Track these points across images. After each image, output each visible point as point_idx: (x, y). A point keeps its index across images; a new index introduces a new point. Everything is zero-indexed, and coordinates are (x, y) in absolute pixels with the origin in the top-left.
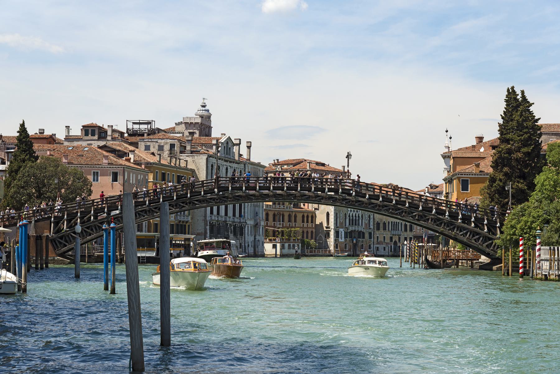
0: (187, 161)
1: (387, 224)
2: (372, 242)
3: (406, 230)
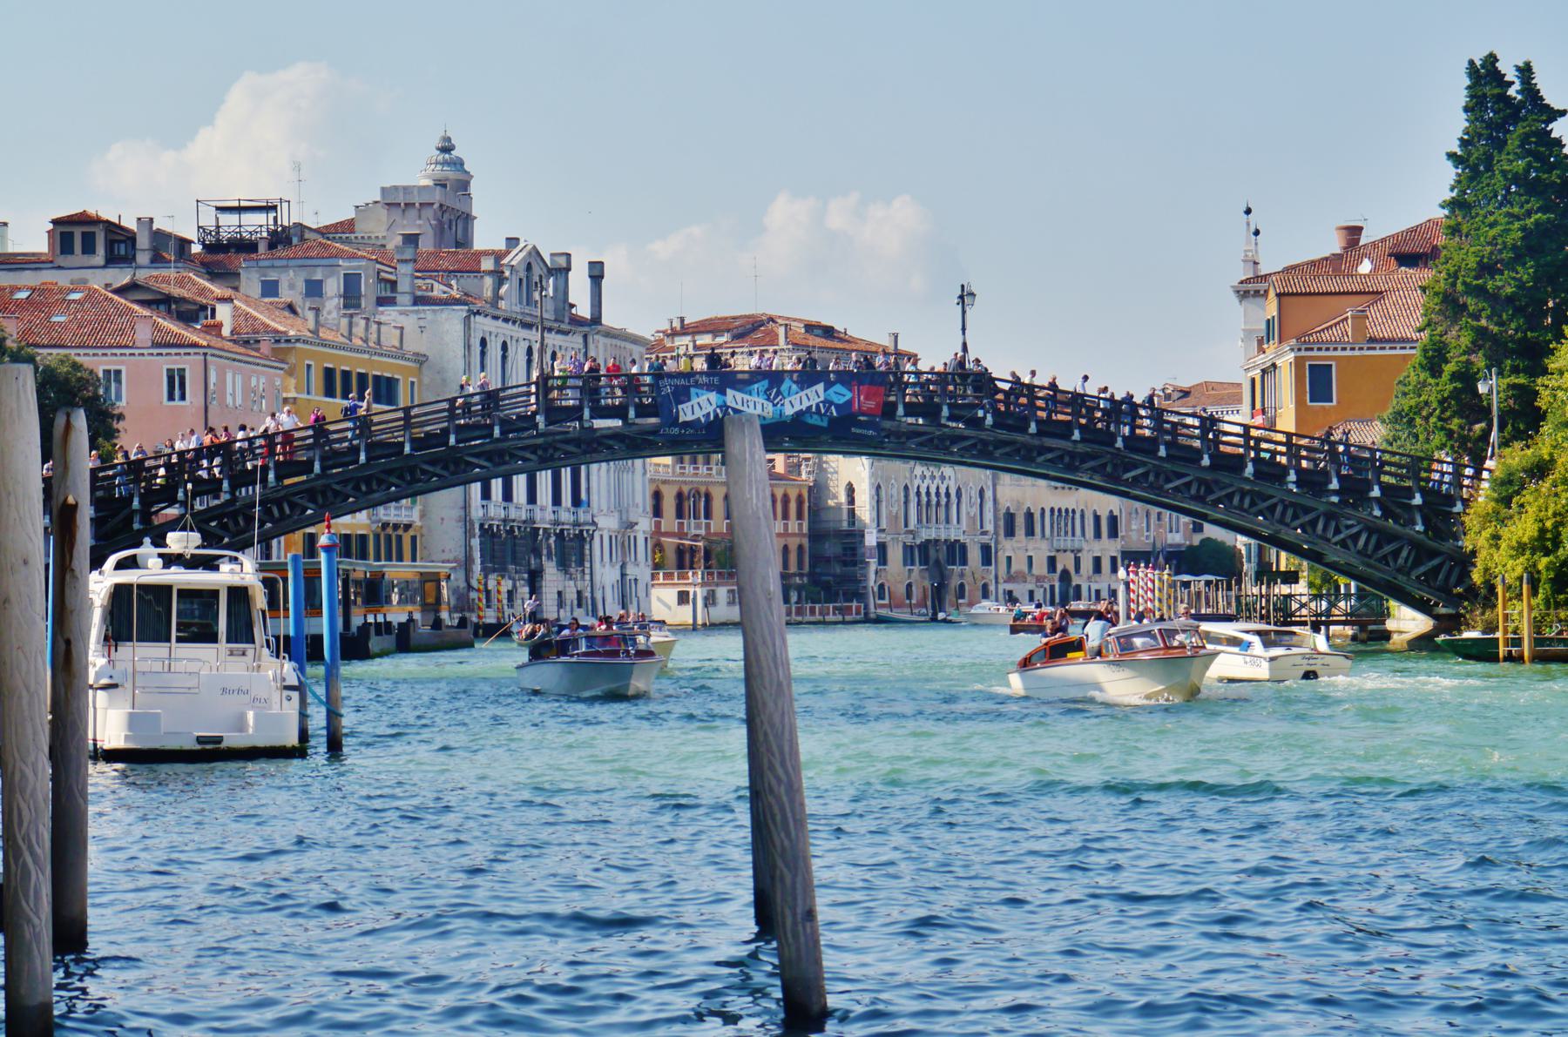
0: (402, 328)
1: (1037, 517)
3: (1098, 535)
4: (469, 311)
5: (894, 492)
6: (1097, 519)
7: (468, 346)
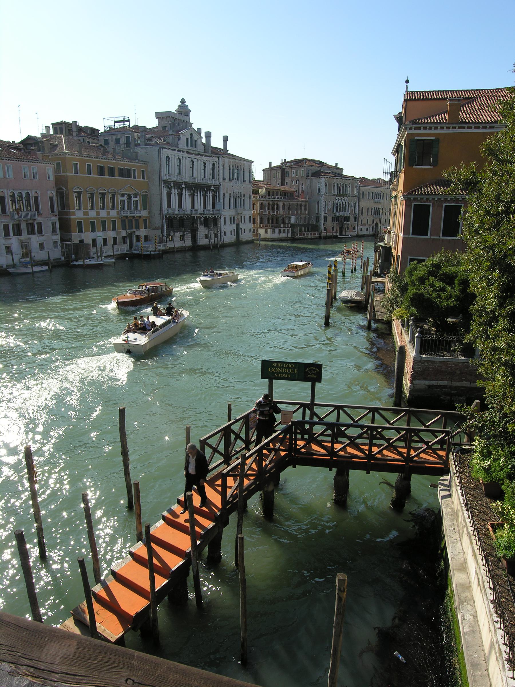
5: (330, 203)
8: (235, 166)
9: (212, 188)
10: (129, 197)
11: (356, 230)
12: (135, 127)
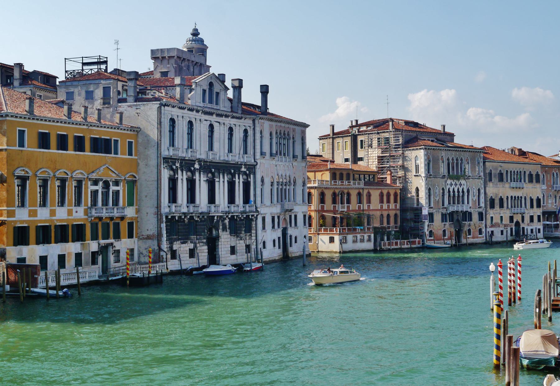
0: (121, 114)
1: (505, 200)
2: (484, 225)
3: (532, 206)
4: (160, 104)
5: (437, 191)
6: (532, 200)
7: (160, 123)
8: (280, 133)
9: (243, 169)
10: (106, 185)
11: (484, 234)
12: (117, 72)
